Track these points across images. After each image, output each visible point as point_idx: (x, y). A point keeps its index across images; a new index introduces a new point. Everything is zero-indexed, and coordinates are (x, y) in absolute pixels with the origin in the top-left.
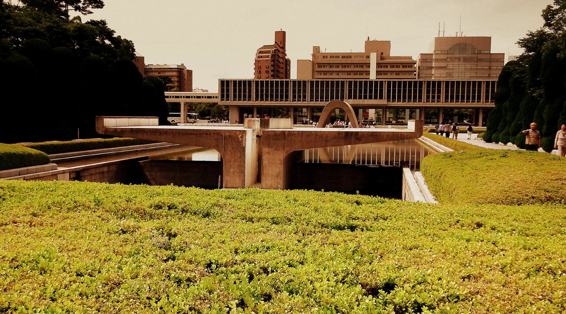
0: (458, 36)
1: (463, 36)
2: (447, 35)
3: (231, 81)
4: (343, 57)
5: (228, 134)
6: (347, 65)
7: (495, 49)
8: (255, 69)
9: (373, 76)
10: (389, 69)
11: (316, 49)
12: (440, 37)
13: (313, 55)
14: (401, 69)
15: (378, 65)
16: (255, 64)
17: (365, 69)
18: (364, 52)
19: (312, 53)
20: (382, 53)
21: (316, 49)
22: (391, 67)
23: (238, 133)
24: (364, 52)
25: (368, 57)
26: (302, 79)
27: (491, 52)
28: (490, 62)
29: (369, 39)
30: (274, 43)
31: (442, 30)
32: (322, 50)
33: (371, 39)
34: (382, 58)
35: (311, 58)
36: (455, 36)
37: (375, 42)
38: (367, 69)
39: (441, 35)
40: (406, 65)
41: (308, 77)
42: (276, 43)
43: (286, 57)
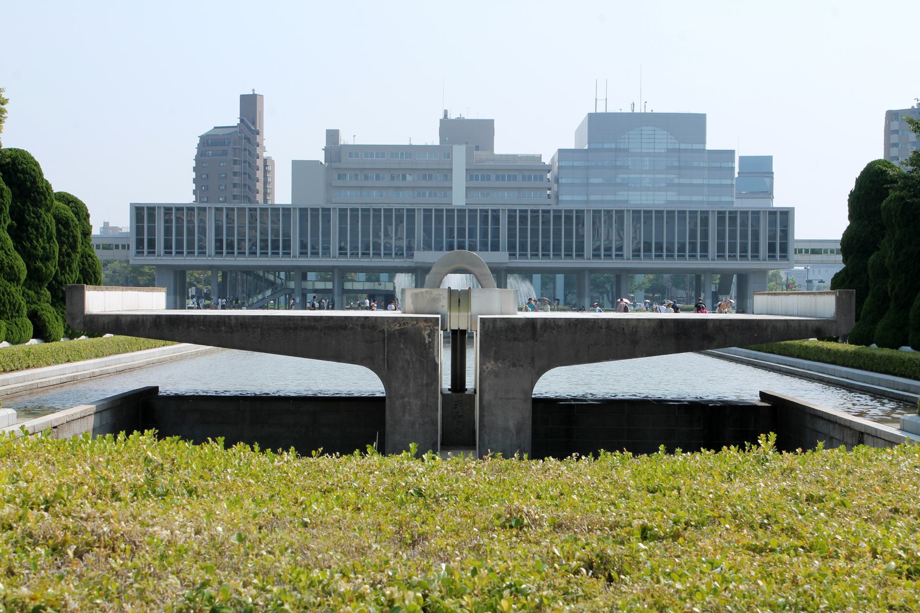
0: (637, 110)
1: (648, 111)
2: (613, 108)
3: (159, 208)
7: (713, 143)
8: (195, 181)
9: (459, 199)
11: (333, 135)
12: (599, 111)
13: (326, 150)
15: (471, 174)
16: (195, 169)
18: (437, 142)
19: (323, 144)
21: (333, 135)
24: (437, 142)
25: (449, 155)
26: (310, 202)
29: (446, 116)
30: (238, 121)
32: (346, 139)
33: (453, 116)
35: (321, 157)
36: (631, 112)
37: (460, 122)
39: (601, 109)
41: (317, 200)
42: (242, 120)
43: (265, 155)
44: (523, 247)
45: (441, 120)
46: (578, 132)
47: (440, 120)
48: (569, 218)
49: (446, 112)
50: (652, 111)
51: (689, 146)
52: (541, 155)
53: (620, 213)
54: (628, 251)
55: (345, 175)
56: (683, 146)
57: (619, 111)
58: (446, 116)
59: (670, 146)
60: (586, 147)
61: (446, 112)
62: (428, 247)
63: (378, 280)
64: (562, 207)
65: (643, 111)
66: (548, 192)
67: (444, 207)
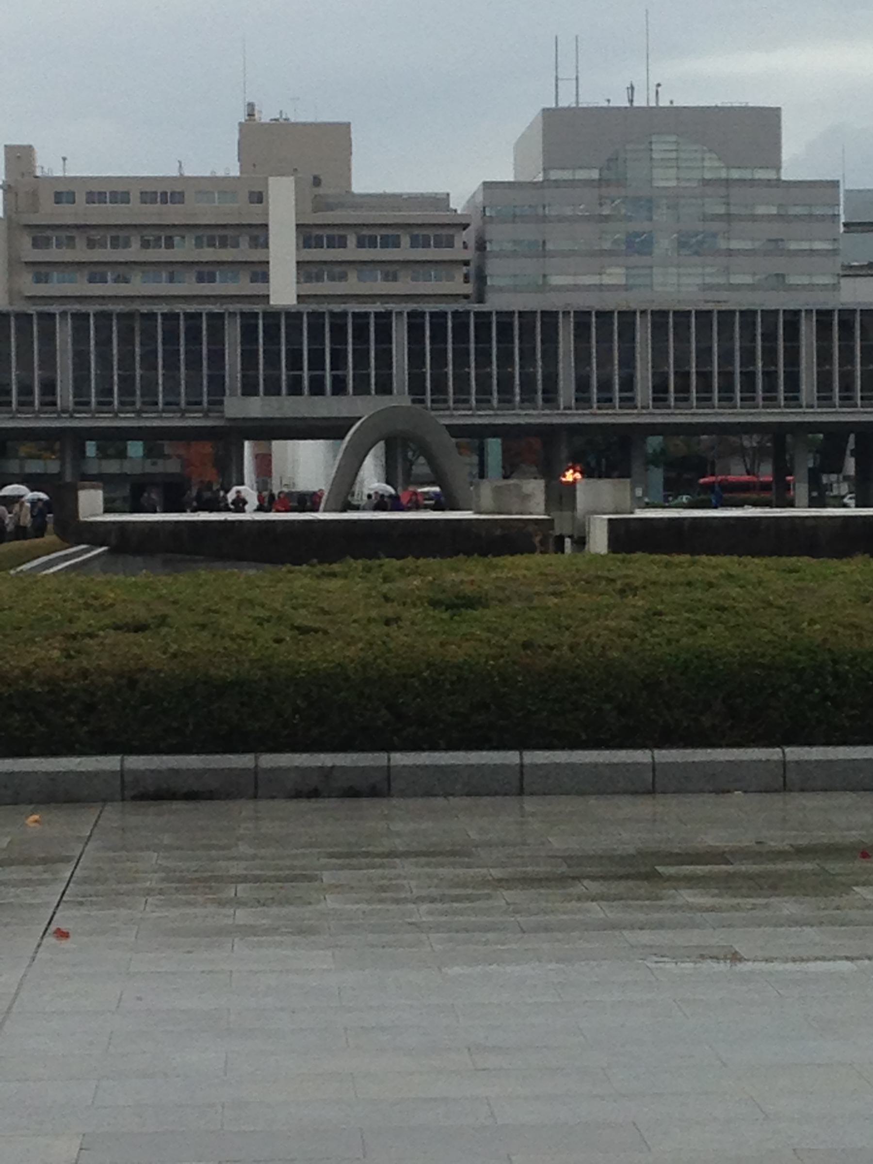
1: (664, 103)
2: (591, 99)
4: (148, 197)
5: (498, 532)
6: (53, 235)
10: (352, 252)
12: (563, 104)
14: (405, 252)
17: (244, 252)
18: (235, 172)
20: (317, 182)
22: (360, 244)
23: (531, 528)
24: (235, 172)
25: (259, 198)
27: (786, 175)
28: (729, 215)
29: (251, 115)
31: (567, 72)
33: (265, 116)
34: (321, 204)
38: (255, 255)
39: (567, 101)
40: (425, 232)
44: (439, 387)
45: (240, 124)
46: (520, 146)
47: (240, 124)
48: (505, 330)
49: (251, 106)
50: (672, 102)
51: (747, 174)
52: (448, 195)
53: (628, 317)
54: (643, 389)
55: (48, 239)
56: (735, 174)
57: (605, 104)
58: (251, 115)
59: (708, 176)
60: (540, 178)
61: (251, 106)
62: (250, 389)
63: (122, 455)
64: (494, 303)
65: (653, 104)
66: (465, 269)
67: (258, 308)
